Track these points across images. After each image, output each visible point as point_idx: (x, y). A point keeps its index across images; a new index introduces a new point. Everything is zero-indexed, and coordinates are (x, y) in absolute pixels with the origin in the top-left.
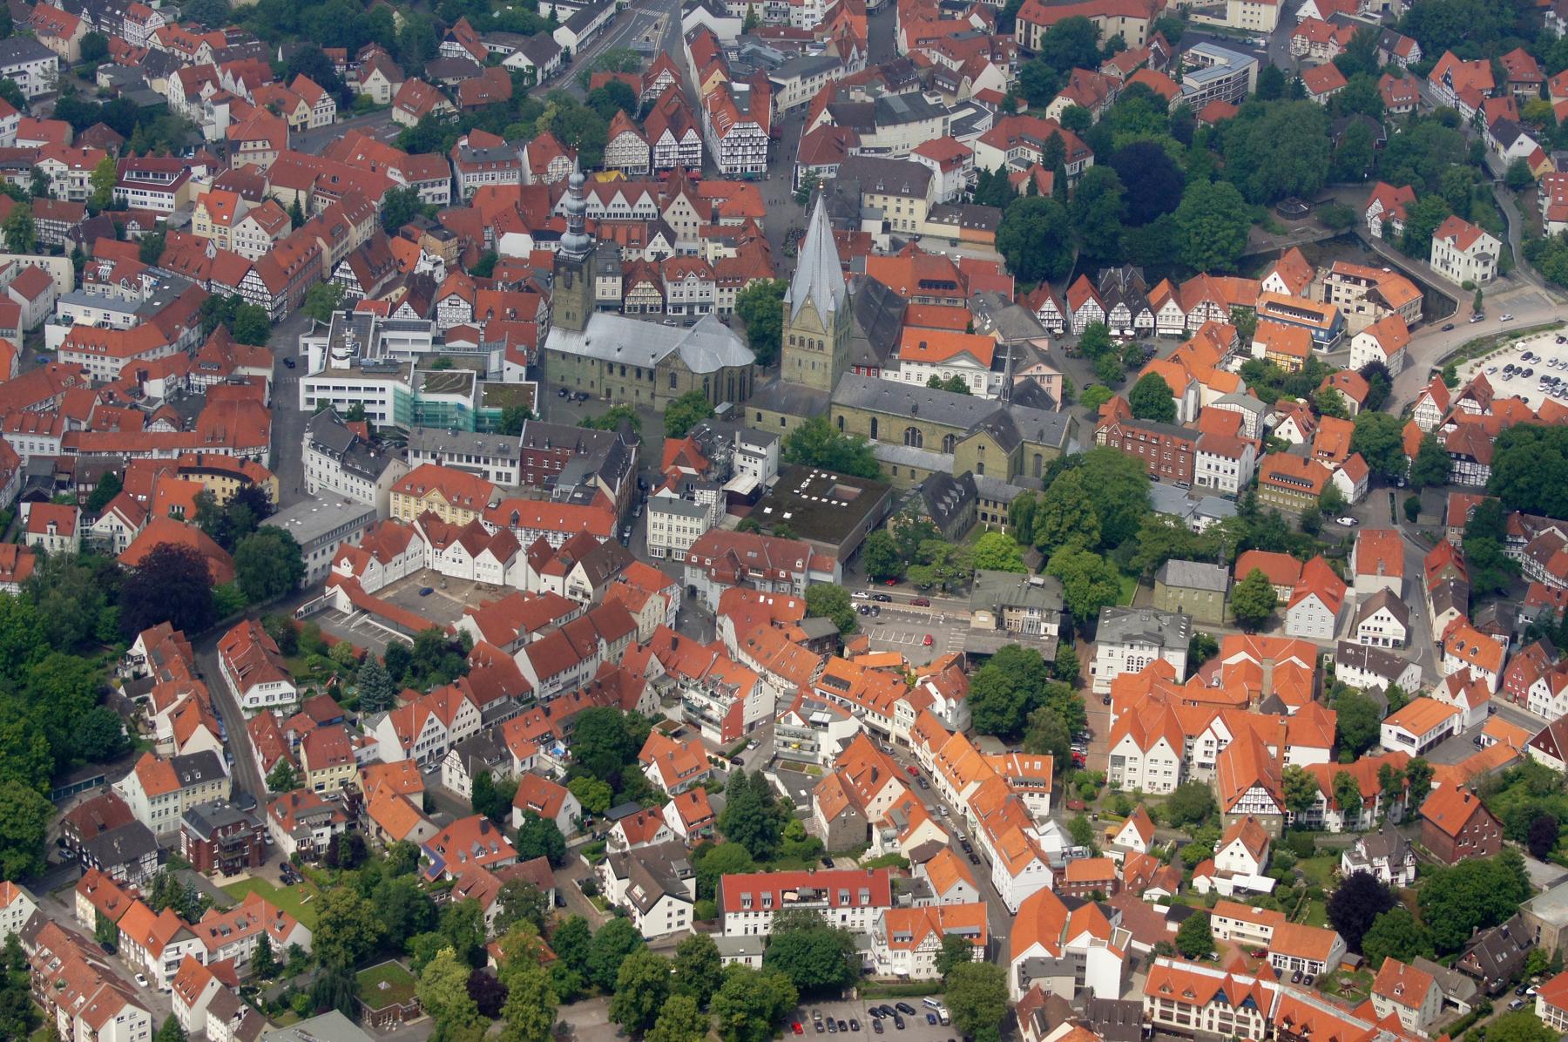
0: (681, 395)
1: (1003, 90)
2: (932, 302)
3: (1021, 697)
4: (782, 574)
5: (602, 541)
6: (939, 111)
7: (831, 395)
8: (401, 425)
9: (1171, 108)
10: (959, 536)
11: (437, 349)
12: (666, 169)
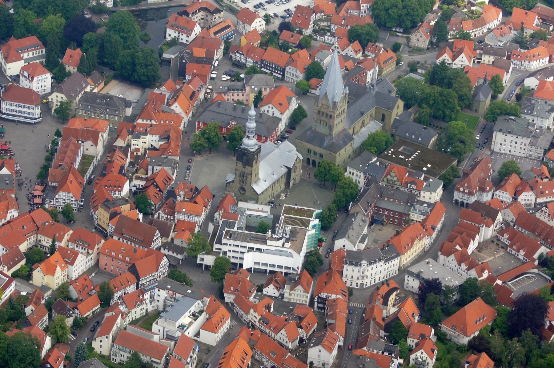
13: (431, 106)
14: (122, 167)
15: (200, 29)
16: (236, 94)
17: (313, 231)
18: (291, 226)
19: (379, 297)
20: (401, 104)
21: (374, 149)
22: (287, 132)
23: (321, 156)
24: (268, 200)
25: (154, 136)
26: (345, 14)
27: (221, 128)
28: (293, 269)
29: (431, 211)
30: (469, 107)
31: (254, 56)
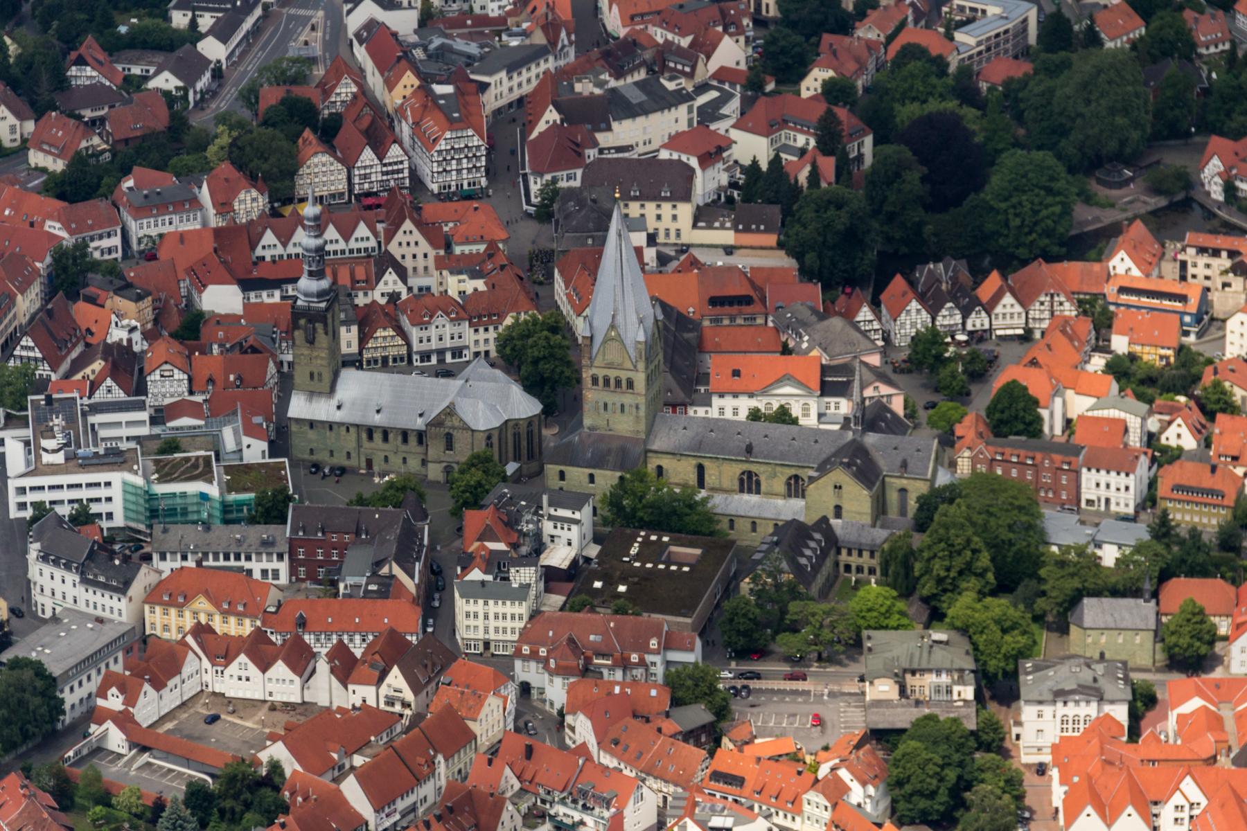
0: (463, 459)
1: (743, 67)
2: (726, 322)
3: (951, 775)
4: (634, 658)
5: (413, 639)
6: (680, 97)
7: (645, 442)
8: (133, 525)
9: (952, 69)
10: (824, 594)
11: (157, 430)
12: (368, 194)
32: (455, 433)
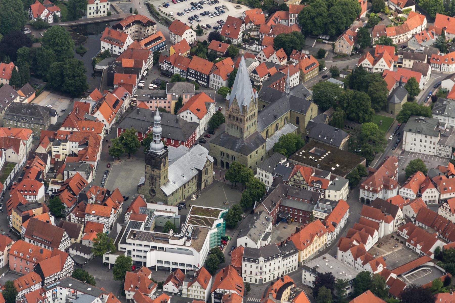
13: (344, 109)
14: (40, 173)
15: (132, 41)
16: (158, 102)
17: (216, 230)
18: (193, 225)
19: (273, 291)
20: (314, 107)
21: (284, 151)
22: (206, 136)
23: (234, 158)
24: (179, 201)
25: (74, 143)
26: (274, 24)
27: (140, 134)
28: (195, 266)
29: (333, 208)
30: (385, 109)
31: (181, 65)
32: (208, 168)
